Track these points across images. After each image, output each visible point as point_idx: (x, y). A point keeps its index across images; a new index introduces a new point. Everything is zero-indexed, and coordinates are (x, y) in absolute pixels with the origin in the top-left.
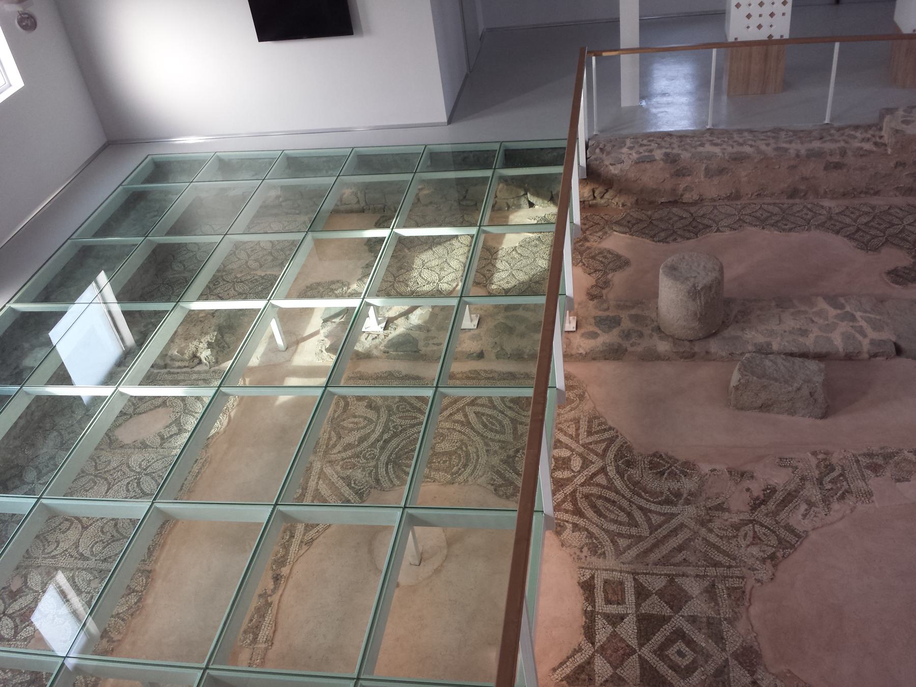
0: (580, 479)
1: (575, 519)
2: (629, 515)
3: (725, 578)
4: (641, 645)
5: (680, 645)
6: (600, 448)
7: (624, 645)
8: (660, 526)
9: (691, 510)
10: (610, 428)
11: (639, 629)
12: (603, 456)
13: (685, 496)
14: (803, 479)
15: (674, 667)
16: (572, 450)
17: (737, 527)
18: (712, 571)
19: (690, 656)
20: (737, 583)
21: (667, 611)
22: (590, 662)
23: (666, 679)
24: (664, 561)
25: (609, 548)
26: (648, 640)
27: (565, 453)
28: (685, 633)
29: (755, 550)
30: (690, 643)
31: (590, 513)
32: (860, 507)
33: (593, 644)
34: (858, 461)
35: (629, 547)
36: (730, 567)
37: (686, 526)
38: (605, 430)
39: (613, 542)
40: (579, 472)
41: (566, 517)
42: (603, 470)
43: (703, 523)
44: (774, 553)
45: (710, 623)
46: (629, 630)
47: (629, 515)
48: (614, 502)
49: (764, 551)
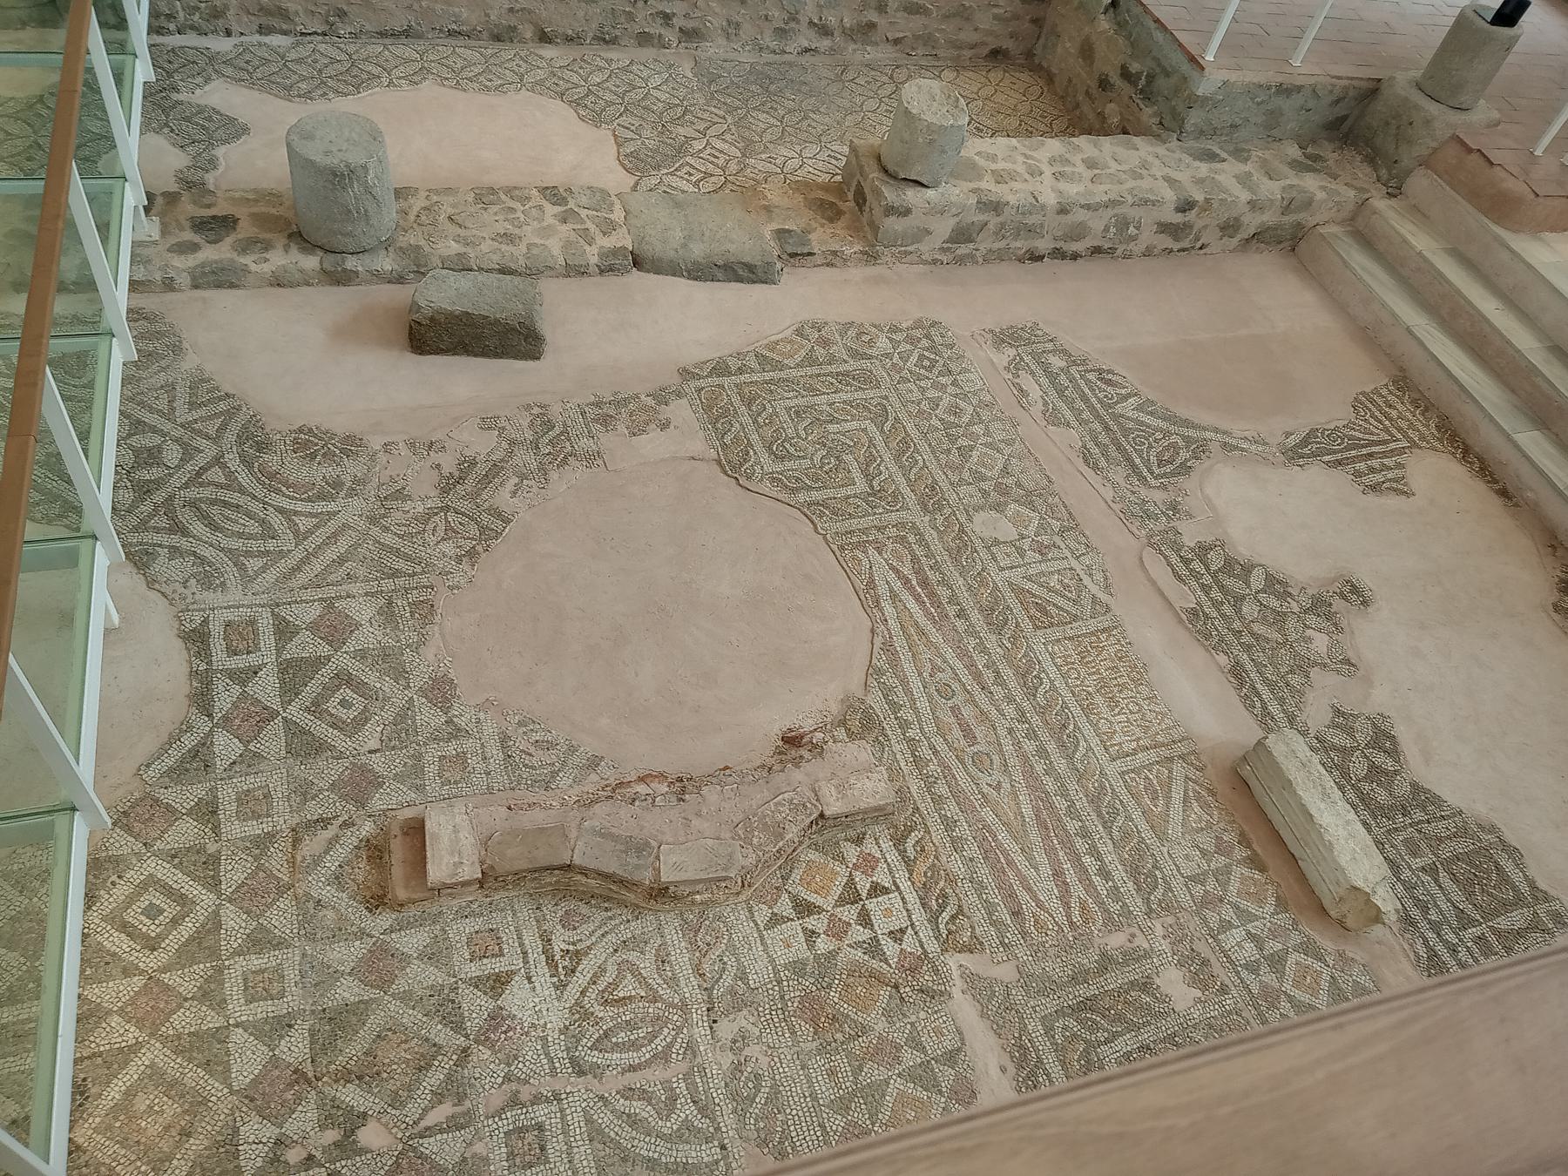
1: (175, 540)
2: (263, 522)
11: (282, 682)
16: (164, 435)
18: (388, 585)
21: (325, 650)
26: (297, 695)
29: (448, 548)
30: (360, 687)
31: (198, 528)
33: (210, 716)
34: (583, 414)
35: (264, 569)
36: (415, 574)
37: (350, 527)
39: (241, 567)
41: (157, 538)
42: (218, 461)
43: (373, 520)
45: (385, 654)
46: (266, 687)
47: (263, 522)
48: (238, 506)
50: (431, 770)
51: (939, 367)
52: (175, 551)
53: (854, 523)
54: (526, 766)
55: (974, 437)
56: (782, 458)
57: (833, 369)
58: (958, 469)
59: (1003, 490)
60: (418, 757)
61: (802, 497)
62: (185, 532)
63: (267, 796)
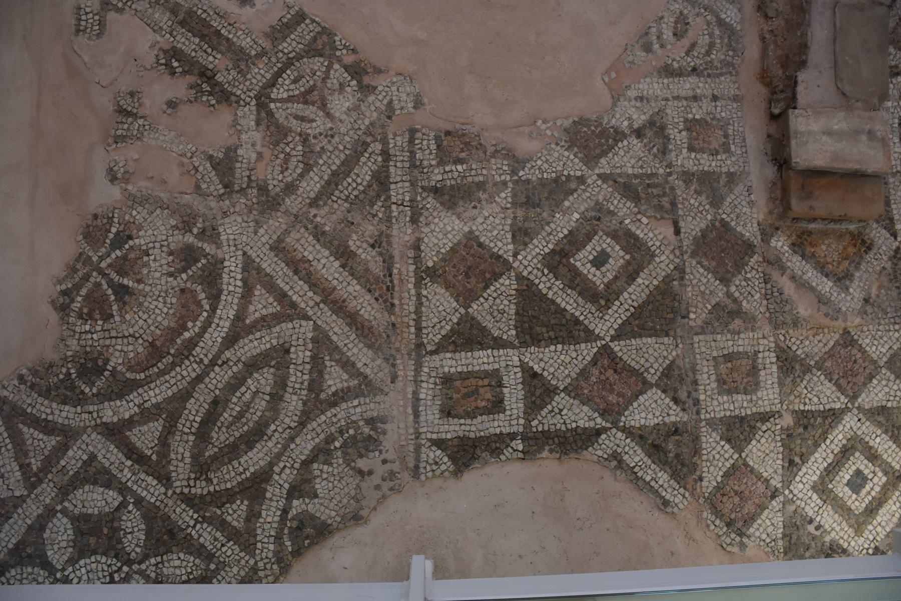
0: (150, 489)
3: (414, 165)
4: (590, 336)
5: (582, 261)
6: (41, 443)
7: (595, 371)
8: (282, 297)
11: (554, 341)
12: (68, 435)
13: (190, 239)
15: (630, 273)
16: (50, 513)
17: (277, 133)
18: (399, 191)
19: (601, 243)
21: (507, 284)
22: (639, 436)
23: (657, 287)
24: (383, 289)
25: (355, 410)
26: (577, 322)
27: (60, 533)
28: (553, 251)
29: (340, 105)
30: (575, 241)
31: (254, 459)
33: (598, 432)
35: (347, 365)
37: (280, 240)
41: (270, 515)
42: (115, 432)
44: (346, 68)
46: (558, 362)
48: (215, 402)
49: (342, 86)
50: (707, 163)
52: (300, 488)
54: (708, 53)
60: (687, 177)
62: (262, 478)
63: (729, 358)
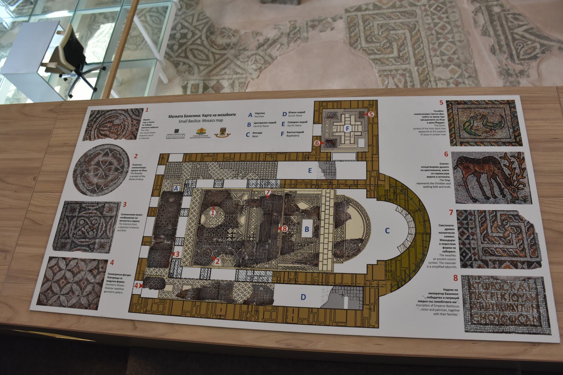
2: (207, 56)
3: (239, 78)
6: (200, 28)
8: (218, 59)
9: (233, 51)
10: (207, 17)
12: (201, 31)
14: (282, 34)
18: (235, 76)
20: (243, 80)
27: (185, 31)
29: (254, 67)
31: (191, 56)
32: (303, 44)
35: (204, 70)
38: (205, 18)
39: (199, 68)
40: (190, 39)
51: (443, 10)
52: (184, 63)
53: (387, 68)
55: (446, 38)
56: (370, 42)
57: (401, 10)
58: (435, 50)
59: (450, 60)
61: (372, 57)
